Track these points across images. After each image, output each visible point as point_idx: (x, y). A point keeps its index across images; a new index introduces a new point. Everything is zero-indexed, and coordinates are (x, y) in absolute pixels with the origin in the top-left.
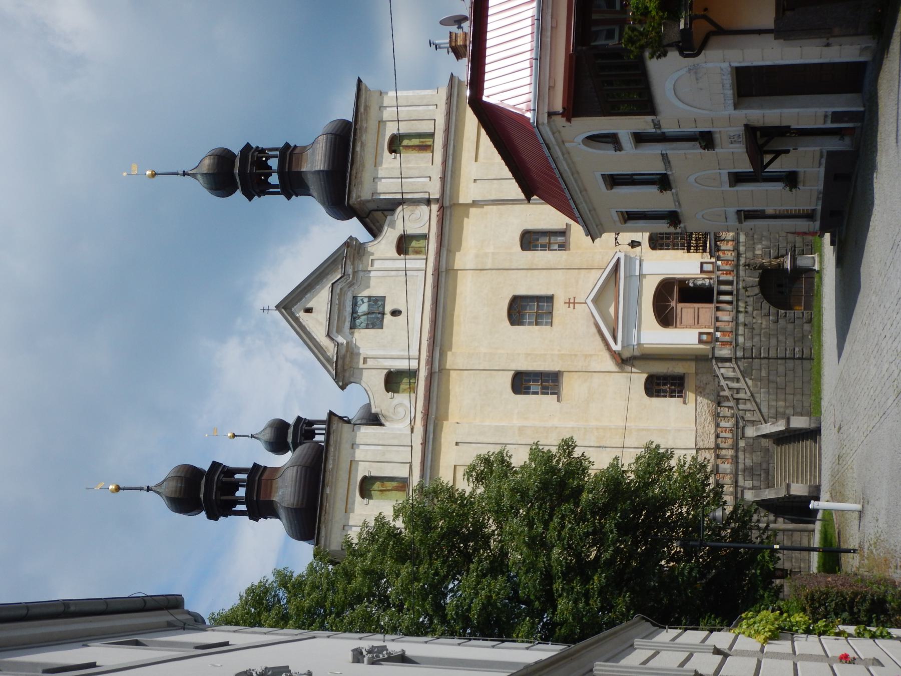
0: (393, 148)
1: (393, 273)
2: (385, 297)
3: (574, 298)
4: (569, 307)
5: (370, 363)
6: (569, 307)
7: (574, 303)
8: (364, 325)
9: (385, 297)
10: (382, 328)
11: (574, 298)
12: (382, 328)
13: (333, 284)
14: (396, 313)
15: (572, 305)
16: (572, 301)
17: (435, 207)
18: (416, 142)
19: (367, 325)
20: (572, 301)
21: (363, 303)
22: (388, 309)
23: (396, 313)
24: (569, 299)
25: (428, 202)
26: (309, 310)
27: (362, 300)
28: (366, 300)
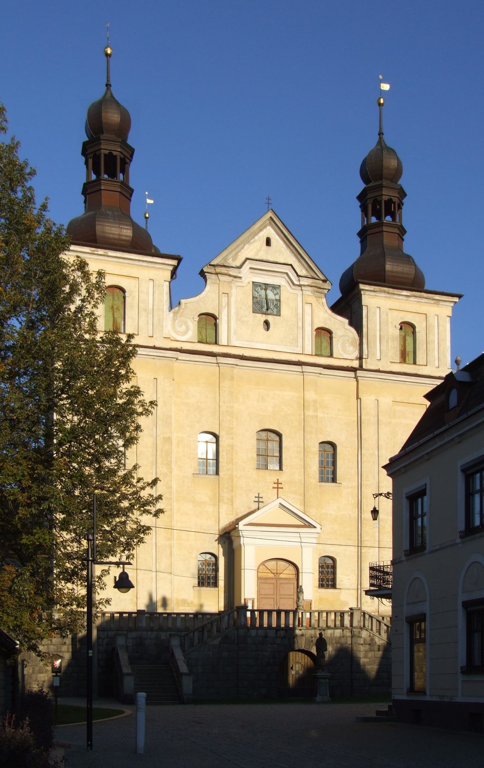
0: (403, 327)
1: (300, 324)
2: (280, 316)
3: (282, 488)
4: (275, 483)
5: (224, 299)
6: (275, 483)
7: (278, 488)
8: (256, 295)
9: (280, 316)
10: (253, 312)
11: (282, 488)
12: (253, 312)
13: (291, 265)
14: (267, 324)
15: (276, 486)
16: (280, 486)
17: (356, 364)
18: (410, 348)
19: (257, 298)
20: (280, 486)
21: (275, 295)
22: (270, 318)
23: (267, 324)
24: (281, 484)
25: (361, 358)
26: (268, 242)
27: (277, 293)
28: (277, 297)
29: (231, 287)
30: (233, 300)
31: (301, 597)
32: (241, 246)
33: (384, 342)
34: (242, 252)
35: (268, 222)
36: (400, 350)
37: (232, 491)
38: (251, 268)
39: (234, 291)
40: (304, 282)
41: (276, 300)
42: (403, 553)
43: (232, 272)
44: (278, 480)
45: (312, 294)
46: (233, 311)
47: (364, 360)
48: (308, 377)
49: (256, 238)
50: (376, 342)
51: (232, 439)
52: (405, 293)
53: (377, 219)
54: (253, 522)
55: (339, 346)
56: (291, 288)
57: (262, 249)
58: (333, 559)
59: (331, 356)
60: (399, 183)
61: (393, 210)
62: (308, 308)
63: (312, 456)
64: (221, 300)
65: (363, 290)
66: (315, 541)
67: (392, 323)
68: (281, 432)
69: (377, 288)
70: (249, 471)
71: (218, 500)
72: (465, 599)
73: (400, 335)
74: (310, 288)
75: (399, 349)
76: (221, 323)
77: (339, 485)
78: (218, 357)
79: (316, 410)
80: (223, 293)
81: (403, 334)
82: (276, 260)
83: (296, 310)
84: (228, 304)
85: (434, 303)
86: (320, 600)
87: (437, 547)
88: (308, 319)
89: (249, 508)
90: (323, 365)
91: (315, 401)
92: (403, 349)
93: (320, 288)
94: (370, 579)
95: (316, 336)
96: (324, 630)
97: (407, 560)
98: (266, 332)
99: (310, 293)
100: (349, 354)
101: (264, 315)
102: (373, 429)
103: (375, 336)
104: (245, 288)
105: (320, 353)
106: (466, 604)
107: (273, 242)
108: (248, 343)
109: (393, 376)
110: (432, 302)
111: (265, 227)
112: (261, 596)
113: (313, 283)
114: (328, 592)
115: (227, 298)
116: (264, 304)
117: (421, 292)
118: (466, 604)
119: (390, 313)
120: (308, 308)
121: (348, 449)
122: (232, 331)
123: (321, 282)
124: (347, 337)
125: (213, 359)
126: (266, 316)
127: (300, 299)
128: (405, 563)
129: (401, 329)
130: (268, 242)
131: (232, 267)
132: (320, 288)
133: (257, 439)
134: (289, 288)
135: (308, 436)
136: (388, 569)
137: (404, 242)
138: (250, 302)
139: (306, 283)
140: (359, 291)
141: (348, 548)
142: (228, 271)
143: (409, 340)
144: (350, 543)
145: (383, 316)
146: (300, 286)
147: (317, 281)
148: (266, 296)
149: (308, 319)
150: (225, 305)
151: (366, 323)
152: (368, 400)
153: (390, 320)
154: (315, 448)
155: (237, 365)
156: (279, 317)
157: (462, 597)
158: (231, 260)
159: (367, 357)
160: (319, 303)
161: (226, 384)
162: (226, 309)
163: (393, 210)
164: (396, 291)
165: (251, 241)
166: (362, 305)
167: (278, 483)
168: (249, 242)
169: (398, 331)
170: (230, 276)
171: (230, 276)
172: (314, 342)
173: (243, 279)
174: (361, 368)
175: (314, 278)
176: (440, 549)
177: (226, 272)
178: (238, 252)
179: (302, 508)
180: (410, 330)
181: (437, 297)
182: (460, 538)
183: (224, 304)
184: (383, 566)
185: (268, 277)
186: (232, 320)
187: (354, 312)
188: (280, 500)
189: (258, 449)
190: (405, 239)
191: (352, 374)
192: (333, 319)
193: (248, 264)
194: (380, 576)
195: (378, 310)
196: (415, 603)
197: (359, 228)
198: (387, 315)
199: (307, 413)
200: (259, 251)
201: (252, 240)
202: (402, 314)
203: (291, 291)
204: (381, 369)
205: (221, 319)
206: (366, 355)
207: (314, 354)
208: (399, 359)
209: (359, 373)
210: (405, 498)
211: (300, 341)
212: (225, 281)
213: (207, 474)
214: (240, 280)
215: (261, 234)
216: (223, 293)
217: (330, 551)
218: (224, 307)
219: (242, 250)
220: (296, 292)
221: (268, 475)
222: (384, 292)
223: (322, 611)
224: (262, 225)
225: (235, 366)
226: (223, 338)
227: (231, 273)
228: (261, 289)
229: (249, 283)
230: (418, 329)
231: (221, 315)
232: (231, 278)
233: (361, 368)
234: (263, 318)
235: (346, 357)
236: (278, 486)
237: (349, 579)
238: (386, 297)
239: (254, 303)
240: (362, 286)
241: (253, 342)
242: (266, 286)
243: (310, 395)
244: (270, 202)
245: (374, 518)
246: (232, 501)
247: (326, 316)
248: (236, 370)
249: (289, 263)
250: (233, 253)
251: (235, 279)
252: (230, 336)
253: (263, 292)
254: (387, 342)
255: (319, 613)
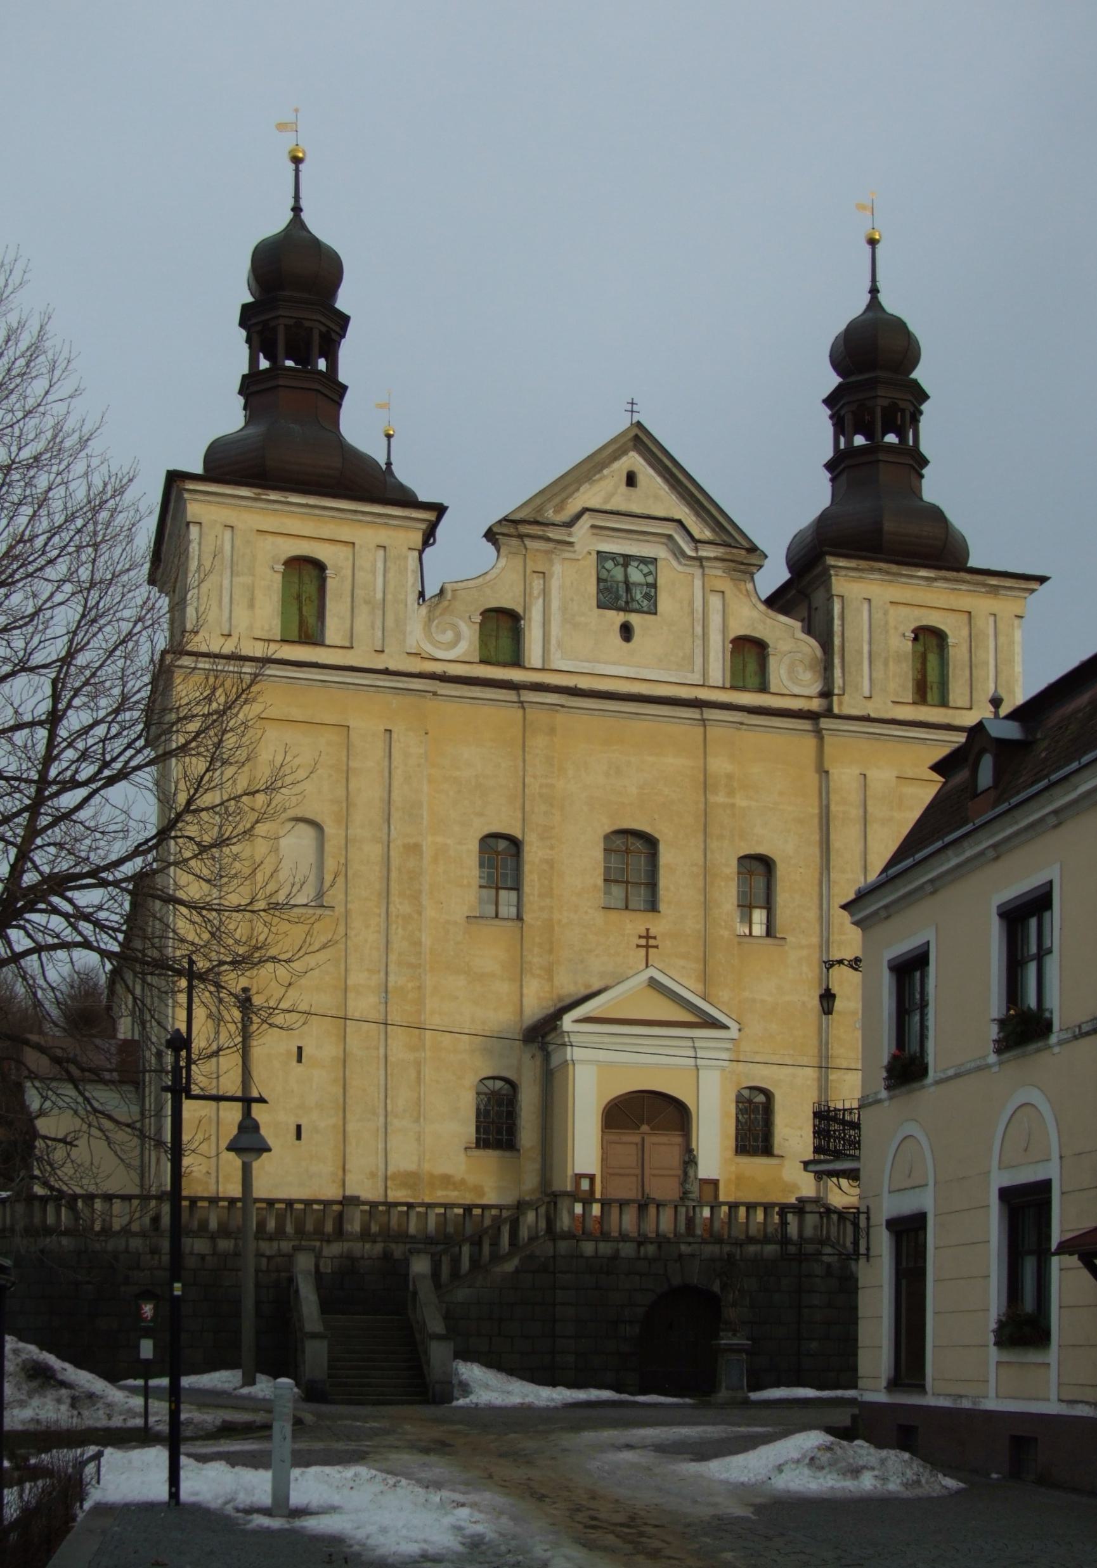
0: (921, 637)
1: (699, 630)
2: (655, 614)
3: (656, 947)
4: (640, 937)
5: (537, 584)
6: (640, 937)
7: (647, 947)
8: (604, 574)
9: (655, 614)
10: (599, 607)
11: (656, 947)
12: (599, 607)
13: (679, 522)
14: (627, 632)
15: (643, 942)
16: (652, 942)
17: (815, 705)
18: (933, 676)
19: (605, 581)
20: (652, 942)
21: (645, 575)
22: (634, 619)
23: (627, 632)
24: (655, 938)
25: (826, 694)
26: (631, 480)
27: (650, 573)
28: (650, 579)
29: (551, 561)
30: (555, 584)
31: (691, 1173)
32: (572, 488)
33: (879, 665)
34: (574, 496)
35: (631, 444)
36: (913, 679)
37: (551, 951)
38: (593, 527)
39: (557, 569)
40: (707, 552)
41: (648, 585)
42: (883, 1084)
43: (552, 533)
44: (648, 930)
45: (725, 575)
46: (555, 605)
47: (835, 698)
48: (714, 732)
49: (605, 472)
50: (861, 663)
51: (552, 848)
52: (923, 573)
53: (867, 440)
54: (591, 1015)
55: (783, 672)
56: (680, 563)
57: (619, 491)
58: (768, 1094)
59: (763, 688)
60: (914, 375)
61: (899, 422)
62: (715, 601)
63: (723, 884)
64: (531, 584)
65: (833, 566)
66: (725, 1055)
67: (896, 628)
68: (657, 835)
69: (863, 564)
70: (586, 912)
71: (519, 970)
72: (1006, 1183)
73: (914, 652)
74: (719, 564)
75: (910, 676)
76: (530, 626)
77: (782, 942)
78: (522, 692)
79: (731, 793)
80: (534, 572)
81: (921, 648)
82: (647, 512)
83: (691, 602)
84: (545, 593)
85: (987, 592)
86: (739, 1180)
87: (951, 1072)
88: (715, 620)
89: (587, 986)
90: (749, 708)
91: (730, 777)
92: (919, 677)
93: (742, 564)
94: (814, 1137)
95: (732, 653)
96: (741, 1245)
97: (891, 1098)
98: (624, 644)
99: (719, 573)
100: (804, 686)
101: (622, 614)
102: (855, 831)
103: (860, 652)
104: (581, 562)
105: (741, 684)
106: (1006, 1194)
107: (641, 479)
108: (586, 664)
109: (897, 729)
110: (984, 590)
111: (625, 452)
112: (611, 1171)
113: (727, 553)
114: (756, 1165)
115: (541, 582)
116: (621, 593)
117: (958, 570)
118: (1006, 1194)
119: (892, 611)
120: (715, 601)
121: (801, 870)
122: (553, 641)
123: (743, 552)
124: (799, 654)
125: (511, 695)
126: (627, 614)
127: (698, 583)
128: (886, 1104)
129: (916, 639)
130: (631, 480)
131: (554, 525)
132: (742, 564)
133: (605, 850)
134: (674, 563)
135: (714, 844)
136: (853, 1115)
137: (924, 481)
138: (592, 588)
139: (712, 555)
140: (827, 568)
141: (799, 1070)
142: (544, 531)
143: (933, 659)
144: (805, 1061)
145: (878, 616)
146: (700, 559)
147: (734, 551)
148: (626, 576)
149: (715, 620)
150: (539, 594)
151: (840, 628)
152: (844, 776)
153: (892, 623)
154: (731, 868)
155: (563, 706)
156: (652, 617)
157: (1001, 1179)
158: (551, 511)
159: (841, 692)
160: (740, 591)
161: (538, 742)
162: (541, 601)
163: (899, 422)
164: (905, 570)
165: (594, 478)
166: (832, 596)
167: (648, 937)
168: (590, 479)
169: (910, 644)
170: (549, 540)
171: (549, 540)
172: (728, 664)
173: (577, 547)
174: (829, 713)
175: (730, 546)
176: (957, 1076)
177: (540, 533)
178: (568, 497)
179: (699, 987)
180: (933, 641)
181: (993, 581)
182: (995, 1052)
183: (536, 593)
184: (844, 1110)
185: (630, 542)
186: (553, 622)
187: (816, 609)
188: (652, 972)
189: (607, 869)
190: (926, 476)
191: (806, 725)
192: (769, 621)
193: (586, 521)
194: (839, 1131)
195: (866, 606)
196: (905, 1189)
197: (828, 454)
198: (886, 613)
199: (712, 798)
200: (610, 496)
201: (597, 476)
202: (917, 612)
203: (680, 568)
204: (873, 715)
205: (530, 619)
206: (839, 687)
207: (728, 685)
208: (911, 696)
209: (825, 723)
210: (888, 970)
211: (698, 661)
212: (537, 550)
213: (497, 916)
214: (571, 549)
215: (616, 465)
216: (534, 572)
217: (761, 1076)
218: (538, 598)
219: (576, 495)
220: (689, 570)
221: (628, 921)
222: (880, 570)
223: (736, 1203)
224: (619, 448)
225: (558, 708)
226: (533, 653)
227: (551, 535)
228: (615, 565)
229: (590, 553)
230: (953, 641)
231: (530, 612)
232: (550, 545)
233: (829, 713)
234: (619, 618)
235: (796, 691)
236: (648, 942)
237: (801, 1136)
238: (882, 580)
239: (599, 591)
240: (831, 561)
241: (599, 662)
242: (627, 560)
243: (720, 765)
244: (635, 408)
245: (826, 1009)
246: (549, 972)
247: (755, 614)
248: (560, 718)
249: (677, 517)
250: (557, 500)
251: (559, 547)
252: (549, 650)
253: (618, 573)
254: (886, 664)
255: (730, 1208)
